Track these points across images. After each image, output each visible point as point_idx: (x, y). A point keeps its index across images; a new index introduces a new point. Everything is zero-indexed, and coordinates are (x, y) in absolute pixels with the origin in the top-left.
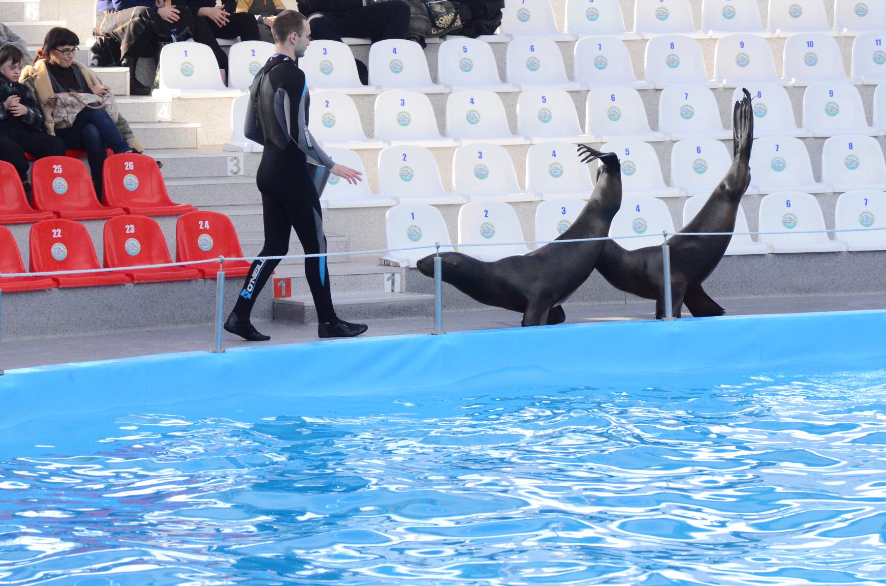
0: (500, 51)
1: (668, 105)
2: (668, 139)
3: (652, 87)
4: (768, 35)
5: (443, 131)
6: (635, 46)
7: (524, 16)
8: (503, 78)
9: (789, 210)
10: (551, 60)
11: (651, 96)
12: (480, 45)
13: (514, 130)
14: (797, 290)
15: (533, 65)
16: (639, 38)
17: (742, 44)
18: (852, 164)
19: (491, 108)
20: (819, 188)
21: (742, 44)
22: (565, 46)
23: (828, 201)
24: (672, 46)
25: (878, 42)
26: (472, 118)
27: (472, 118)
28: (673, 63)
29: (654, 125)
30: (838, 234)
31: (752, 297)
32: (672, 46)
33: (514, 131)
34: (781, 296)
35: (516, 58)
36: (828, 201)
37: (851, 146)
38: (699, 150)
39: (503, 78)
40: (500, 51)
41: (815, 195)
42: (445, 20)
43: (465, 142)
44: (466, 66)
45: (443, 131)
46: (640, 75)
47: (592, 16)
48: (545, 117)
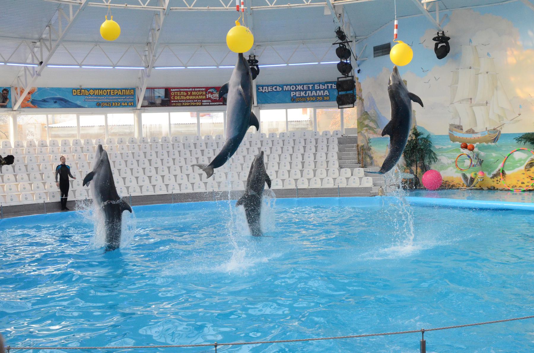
0: (14, 167)
5: (3, 182)
6: (39, 166)
7: (18, 161)
8: (14, 172)
10: (23, 169)
11: (42, 174)
12: (9, 167)
13: (16, 181)
15: (20, 169)
19: (26, 177)
22: (26, 166)
26: (9, 179)
27: (9, 179)
28: (46, 168)
33: (16, 181)
35: (17, 168)
39: (14, 172)
40: (14, 167)
42: (3, 162)
43: (21, 183)
44: (7, 170)
45: (3, 182)
46: (40, 170)
47: (31, 160)
48: (22, 179)
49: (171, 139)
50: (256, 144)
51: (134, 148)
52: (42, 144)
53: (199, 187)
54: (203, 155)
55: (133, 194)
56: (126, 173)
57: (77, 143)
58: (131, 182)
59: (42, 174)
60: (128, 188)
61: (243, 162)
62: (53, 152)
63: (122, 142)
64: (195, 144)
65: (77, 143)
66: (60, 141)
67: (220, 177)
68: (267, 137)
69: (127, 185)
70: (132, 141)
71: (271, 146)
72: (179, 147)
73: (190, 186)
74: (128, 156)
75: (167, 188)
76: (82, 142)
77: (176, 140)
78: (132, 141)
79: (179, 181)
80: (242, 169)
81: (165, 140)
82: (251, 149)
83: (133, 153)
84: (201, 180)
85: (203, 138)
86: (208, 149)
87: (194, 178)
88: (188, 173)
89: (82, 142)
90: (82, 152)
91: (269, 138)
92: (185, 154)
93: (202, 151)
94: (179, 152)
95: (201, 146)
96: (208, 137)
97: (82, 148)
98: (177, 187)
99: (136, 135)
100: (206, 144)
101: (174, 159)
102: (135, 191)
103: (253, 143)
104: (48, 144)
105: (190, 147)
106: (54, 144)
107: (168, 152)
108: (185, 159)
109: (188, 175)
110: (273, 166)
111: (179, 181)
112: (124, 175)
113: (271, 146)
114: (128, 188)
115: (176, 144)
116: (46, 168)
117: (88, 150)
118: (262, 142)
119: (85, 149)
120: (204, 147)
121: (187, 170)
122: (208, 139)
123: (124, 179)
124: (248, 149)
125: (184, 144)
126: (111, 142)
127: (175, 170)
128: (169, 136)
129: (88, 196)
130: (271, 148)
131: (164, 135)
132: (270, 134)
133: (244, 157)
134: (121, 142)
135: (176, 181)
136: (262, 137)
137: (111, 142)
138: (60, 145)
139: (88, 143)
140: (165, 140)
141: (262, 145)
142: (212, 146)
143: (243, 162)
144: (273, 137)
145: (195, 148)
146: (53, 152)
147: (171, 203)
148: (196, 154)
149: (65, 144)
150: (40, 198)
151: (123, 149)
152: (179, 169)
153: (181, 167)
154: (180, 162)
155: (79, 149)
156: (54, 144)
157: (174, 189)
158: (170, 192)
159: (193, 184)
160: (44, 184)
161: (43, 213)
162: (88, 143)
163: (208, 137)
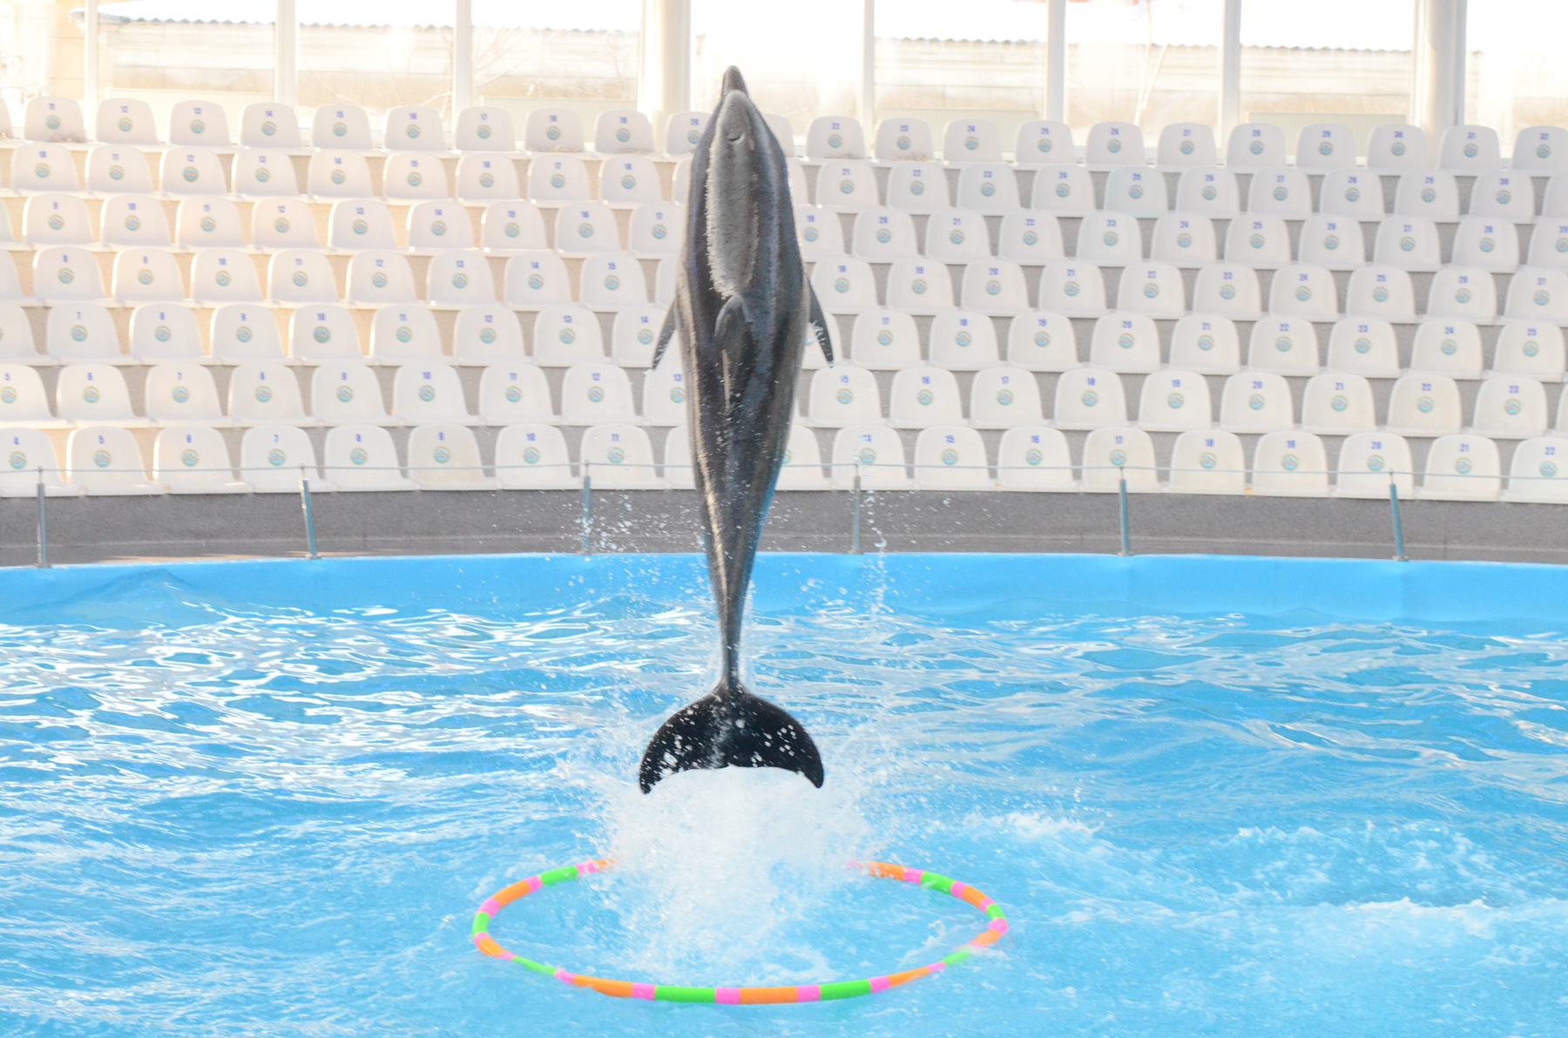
1: (58, 329)
2: (55, 363)
3: (40, 304)
4: (178, 250)
9: (189, 446)
11: (38, 316)
14: (197, 536)
16: (27, 249)
17: (145, 260)
18: (264, 396)
20: (226, 422)
21: (145, 260)
23: (233, 437)
24: (65, 259)
25: (299, 261)
28: (66, 277)
29: (41, 347)
30: (244, 474)
31: (145, 542)
32: (65, 259)
34: (177, 541)
36: (233, 437)
37: (262, 376)
38: (90, 377)
41: (221, 430)
46: (28, 290)
49: (870, 139)
50: (1428, 197)
51: (628, 184)
52: (53, 124)
53: (1034, 460)
54: (1070, 251)
55: (606, 478)
56: (567, 338)
57: (269, 130)
58: (596, 396)
59: (38, 316)
60: (573, 435)
61: (1329, 311)
62: (116, 174)
63: (553, 135)
64: (1025, 178)
65: (269, 130)
66: (161, 110)
67: (1176, 402)
68: (1506, 152)
69: (570, 417)
70: (623, 136)
71: (1527, 214)
72: (917, 190)
73: (973, 449)
74: (586, 232)
75: (826, 455)
76: (306, 120)
77: (904, 144)
78: (623, 136)
79: (907, 411)
80: (1323, 361)
81: (835, 142)
82: (1391, 230)
83: (622, 215)
84: (1048, 413)
85: (1080, 138)
86: (1106, 214)
87: (1005, 399)
88: (964, 359)
89: (306, 120)
90: (302, 189)
91: (1517, 162)
92: (957, 239)
93: (1070, 223)
94: (920, 220)
95: (1063, 192)
96: (1114, 137)
97: (300, 162)
98: (890, 448)
99: (650, 102)
100: (1099, 178)
101: (881, 270)
102: (616, 459)
103: (1408, 191)
104: (90, 128)
105: (988, 191)
106: (125, 127)
107: (847, 219)
108: (956, 269)
109: (964, 377)
110: (1530, 351)
111: (907, 411)
112: (556, 354)
113: (1527, 214)
114: (573, 435)
115: (902, 171)
116: (66, 277)
117: (338, 178)
118: (1465, 183)
119: (322, 165)
120: (1080, 201)
121: (963, 341)
122: (1114, 148)
123: (555, 374)
124: (1369, 227)
125: (952, 174)
126: (484, 133)
127: (885, 339)
128: (863, 118)
129: (322, 475)
130: (1524, 230)
131: (827, 107)
132: (1522, 138)
133: (1342, 276)
134: (551, 137)
135: (885, 412)
136: (1470, 152)
137: (484, 133)
138: (164, 133)
139: (340, 131)
140: (835, 142)
141: (1464, 209)
142: (1136, 193)
143: (1329, 311)
144: (1543, 153)
145: (1025, 202)
146: (116, 174)
147: (841, 546)
148: (1030, 240)
149: (198, 128)
150: (18, 463)
151: (558, 183)
152: (906, 334)
153: (924, 322)
154: (919, 288)
155: (280, 166)
156: (125, 126)
157: (867, 459)
158: (842, 480)
159: (992, 436)
160: (49, 375)
161: (30, 558)
162: (340, 131)
163: (1114, 137)
